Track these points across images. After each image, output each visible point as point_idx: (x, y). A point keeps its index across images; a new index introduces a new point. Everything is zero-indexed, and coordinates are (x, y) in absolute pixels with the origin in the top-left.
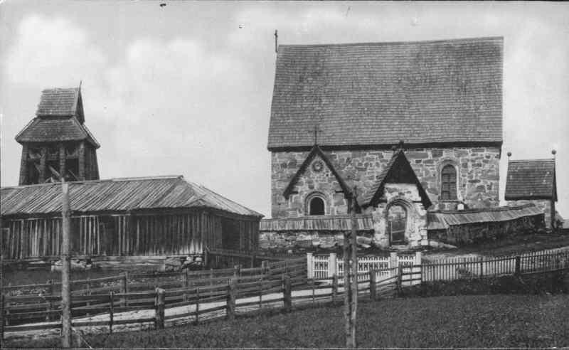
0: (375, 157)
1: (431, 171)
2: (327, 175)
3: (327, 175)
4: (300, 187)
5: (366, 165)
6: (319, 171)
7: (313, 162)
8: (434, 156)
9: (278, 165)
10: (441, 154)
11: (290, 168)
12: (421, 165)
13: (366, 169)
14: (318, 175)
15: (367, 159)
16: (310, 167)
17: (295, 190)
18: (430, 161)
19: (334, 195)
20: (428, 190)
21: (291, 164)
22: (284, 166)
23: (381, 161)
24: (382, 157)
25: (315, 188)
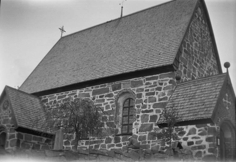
0: (71, 96)
1: (110, 105)
10: (119, 87)
19: (11, 129)
20: (152, 124)
24: (76, 96)
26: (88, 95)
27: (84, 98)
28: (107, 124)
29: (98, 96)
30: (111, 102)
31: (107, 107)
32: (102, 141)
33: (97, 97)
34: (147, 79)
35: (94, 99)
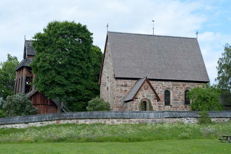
0: (160, 84)
1: (182, 92)
2: (150, 91)
3: (150, 91)
5: (156, 88)
6: (146, 89)
7: (144, 86)
8: (183, 85)
10: (185, 85)
13: (156, 90)
14: (146, 91)
15: (157, 85)
16: (143, 88)
17: (137, 97)
18: (181, 88)
19: (153, 100)
21: (125, 85)
22: (122, 86)
23: (162, 86)
24: (163, 85)
25: (145, 97)
26: (170, 86)
27: (168, 86)
28: (181, 100)
29: (175, 87)
30: (182, 91)
31: (180, 93)
32: (45, 111)
33: (175, 87)
34: (198, 84)
35: (173, 88)
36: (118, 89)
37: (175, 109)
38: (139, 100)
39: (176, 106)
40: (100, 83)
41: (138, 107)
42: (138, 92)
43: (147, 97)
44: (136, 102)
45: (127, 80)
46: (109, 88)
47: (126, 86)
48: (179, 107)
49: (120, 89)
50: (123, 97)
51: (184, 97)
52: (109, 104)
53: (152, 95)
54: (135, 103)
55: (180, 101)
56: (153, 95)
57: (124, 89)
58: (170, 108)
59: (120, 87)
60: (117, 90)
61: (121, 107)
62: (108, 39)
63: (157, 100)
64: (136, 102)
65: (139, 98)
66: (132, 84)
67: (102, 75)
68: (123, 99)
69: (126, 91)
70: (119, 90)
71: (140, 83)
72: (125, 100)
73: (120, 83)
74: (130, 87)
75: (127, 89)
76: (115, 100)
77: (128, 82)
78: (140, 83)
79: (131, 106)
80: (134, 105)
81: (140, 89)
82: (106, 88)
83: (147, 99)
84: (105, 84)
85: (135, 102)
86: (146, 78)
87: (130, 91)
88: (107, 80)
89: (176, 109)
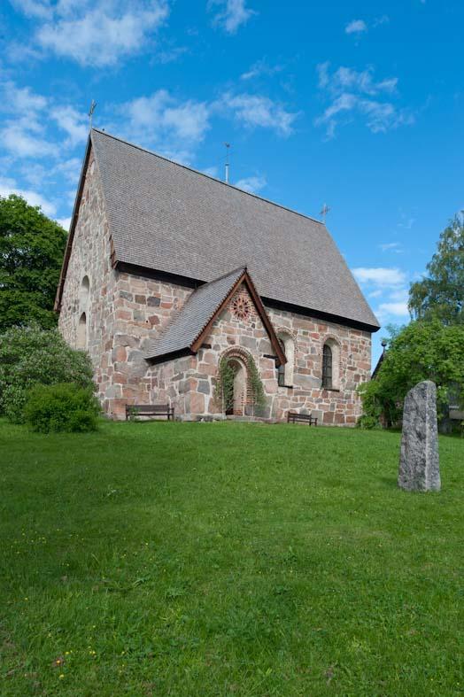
2: (253, 326)
3: (253, 326)
4: (213, 336)
6: (240, 316)
8: (320, 330)
9: (131, 295)
10: (325, 330)
11: (149, 305)
12: (308, 340)
14: (241, 323)
18: (315, 336)
19: (261, 360)
21: (151, 299)
22: (140, 299)
25: (237, 344)
26: (288, 324)
29: (302, 330)
33: (301, 332)
35: (296, 332)
36: (125, 308)
37: (299, 397)
38: (213, 357)
39: (301, 390)
40: (60, 306)
41: (209, 380)
42: (211, 324)
43: (244, 345)
44: (202, 362)
45: (160, 284)
46: (87, 315)
47: (154, 301)
48: (308, 394)
49: (131, 311)
50: (142, 341)
51: (321, 364)
52: (88, 361)
53: (259, 340)
54: (199, 363)
55: (312, 375)
56: (262, 341)
57: (147, 312)
58: (286, 394)
59: (134, 301)
60: (122, 315)
61: (136, 381)
62: (94, 149)
63: (273, 361)
64: (202, 362)
65: (217, 347)
66: (176, 300)
67: (67, 280)
68: (142, 349)
69: (154, 320)
70: (129, 314)
71: (208, 299)
72: (153, 354)
73: (133, 290)
74: (169, 311)
75: (158, 313)
76: (110, 352)
77: (165, 291)
78: (208, 299)
79: (181, 376)
80: (196, 371)
81: (220, 312)
82: (77, 318)
83: (243, 354)
84: (73, 305)
85: (200, 359)
86: (242, 271)
87: (171, 322)
88: (83, 289)
89: (301, 399)
